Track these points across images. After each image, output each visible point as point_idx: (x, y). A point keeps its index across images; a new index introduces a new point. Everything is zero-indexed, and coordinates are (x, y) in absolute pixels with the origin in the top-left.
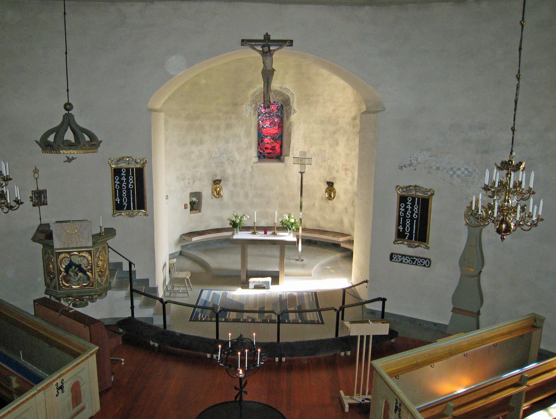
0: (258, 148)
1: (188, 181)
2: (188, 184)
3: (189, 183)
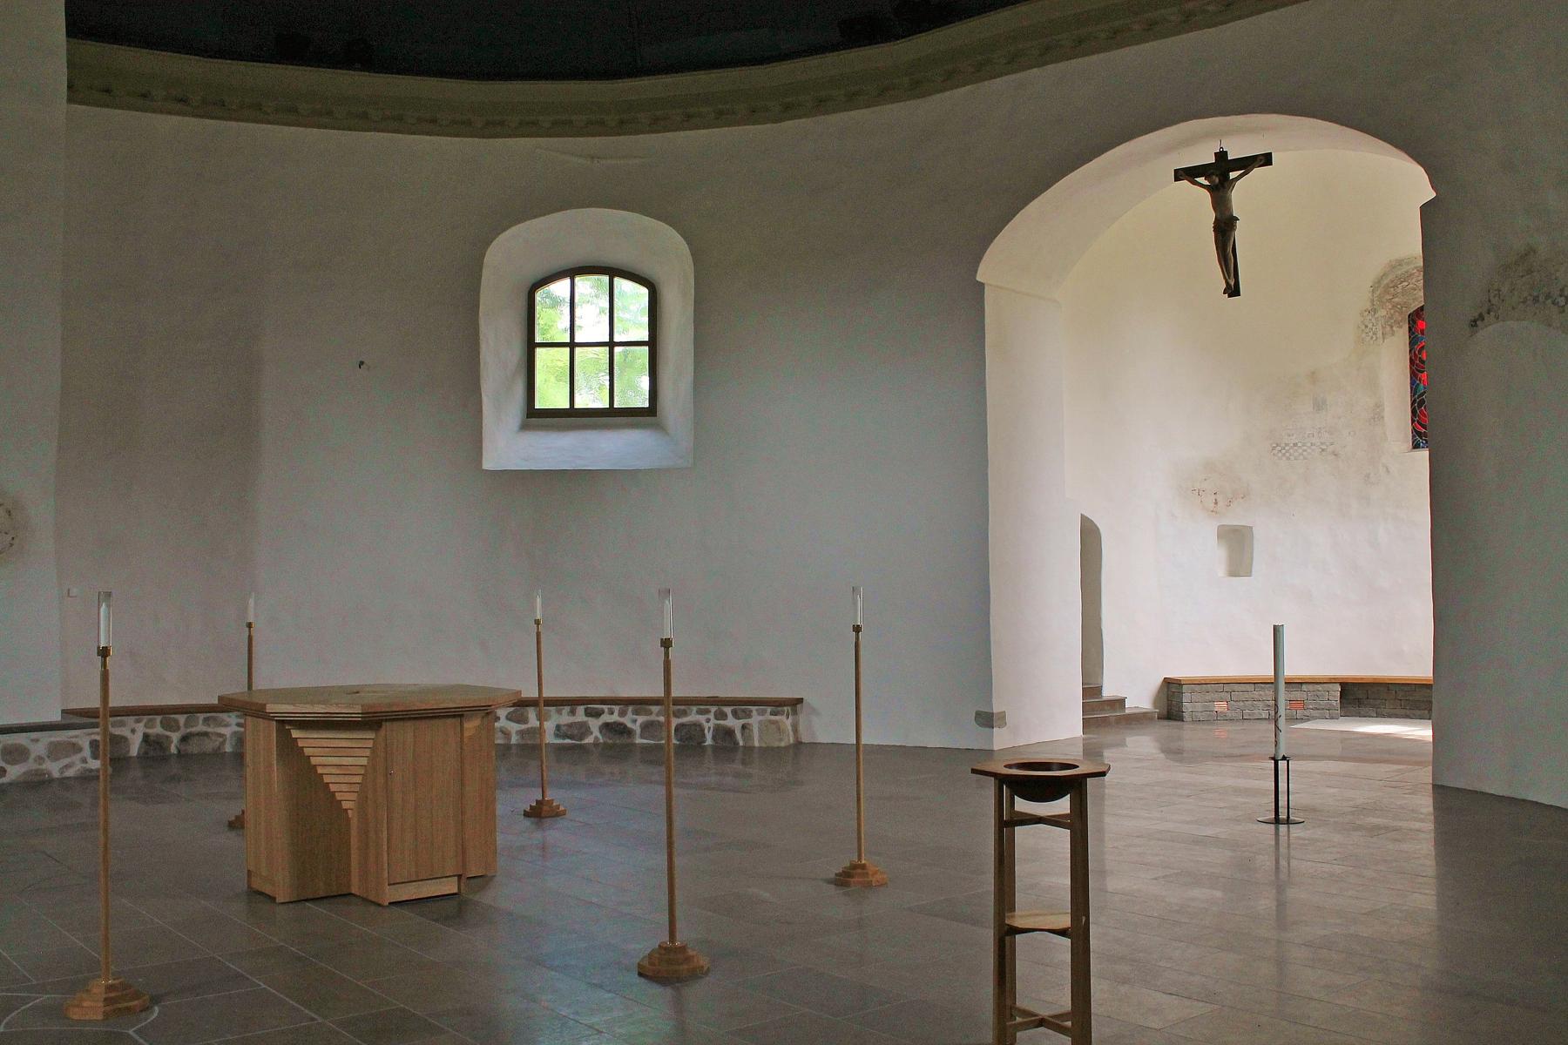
0: (1413, 421)
1: (1214, 497)
2: (1213, 505)
3: (1216, 503)
